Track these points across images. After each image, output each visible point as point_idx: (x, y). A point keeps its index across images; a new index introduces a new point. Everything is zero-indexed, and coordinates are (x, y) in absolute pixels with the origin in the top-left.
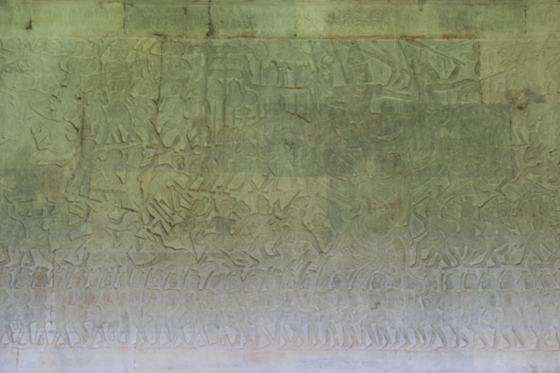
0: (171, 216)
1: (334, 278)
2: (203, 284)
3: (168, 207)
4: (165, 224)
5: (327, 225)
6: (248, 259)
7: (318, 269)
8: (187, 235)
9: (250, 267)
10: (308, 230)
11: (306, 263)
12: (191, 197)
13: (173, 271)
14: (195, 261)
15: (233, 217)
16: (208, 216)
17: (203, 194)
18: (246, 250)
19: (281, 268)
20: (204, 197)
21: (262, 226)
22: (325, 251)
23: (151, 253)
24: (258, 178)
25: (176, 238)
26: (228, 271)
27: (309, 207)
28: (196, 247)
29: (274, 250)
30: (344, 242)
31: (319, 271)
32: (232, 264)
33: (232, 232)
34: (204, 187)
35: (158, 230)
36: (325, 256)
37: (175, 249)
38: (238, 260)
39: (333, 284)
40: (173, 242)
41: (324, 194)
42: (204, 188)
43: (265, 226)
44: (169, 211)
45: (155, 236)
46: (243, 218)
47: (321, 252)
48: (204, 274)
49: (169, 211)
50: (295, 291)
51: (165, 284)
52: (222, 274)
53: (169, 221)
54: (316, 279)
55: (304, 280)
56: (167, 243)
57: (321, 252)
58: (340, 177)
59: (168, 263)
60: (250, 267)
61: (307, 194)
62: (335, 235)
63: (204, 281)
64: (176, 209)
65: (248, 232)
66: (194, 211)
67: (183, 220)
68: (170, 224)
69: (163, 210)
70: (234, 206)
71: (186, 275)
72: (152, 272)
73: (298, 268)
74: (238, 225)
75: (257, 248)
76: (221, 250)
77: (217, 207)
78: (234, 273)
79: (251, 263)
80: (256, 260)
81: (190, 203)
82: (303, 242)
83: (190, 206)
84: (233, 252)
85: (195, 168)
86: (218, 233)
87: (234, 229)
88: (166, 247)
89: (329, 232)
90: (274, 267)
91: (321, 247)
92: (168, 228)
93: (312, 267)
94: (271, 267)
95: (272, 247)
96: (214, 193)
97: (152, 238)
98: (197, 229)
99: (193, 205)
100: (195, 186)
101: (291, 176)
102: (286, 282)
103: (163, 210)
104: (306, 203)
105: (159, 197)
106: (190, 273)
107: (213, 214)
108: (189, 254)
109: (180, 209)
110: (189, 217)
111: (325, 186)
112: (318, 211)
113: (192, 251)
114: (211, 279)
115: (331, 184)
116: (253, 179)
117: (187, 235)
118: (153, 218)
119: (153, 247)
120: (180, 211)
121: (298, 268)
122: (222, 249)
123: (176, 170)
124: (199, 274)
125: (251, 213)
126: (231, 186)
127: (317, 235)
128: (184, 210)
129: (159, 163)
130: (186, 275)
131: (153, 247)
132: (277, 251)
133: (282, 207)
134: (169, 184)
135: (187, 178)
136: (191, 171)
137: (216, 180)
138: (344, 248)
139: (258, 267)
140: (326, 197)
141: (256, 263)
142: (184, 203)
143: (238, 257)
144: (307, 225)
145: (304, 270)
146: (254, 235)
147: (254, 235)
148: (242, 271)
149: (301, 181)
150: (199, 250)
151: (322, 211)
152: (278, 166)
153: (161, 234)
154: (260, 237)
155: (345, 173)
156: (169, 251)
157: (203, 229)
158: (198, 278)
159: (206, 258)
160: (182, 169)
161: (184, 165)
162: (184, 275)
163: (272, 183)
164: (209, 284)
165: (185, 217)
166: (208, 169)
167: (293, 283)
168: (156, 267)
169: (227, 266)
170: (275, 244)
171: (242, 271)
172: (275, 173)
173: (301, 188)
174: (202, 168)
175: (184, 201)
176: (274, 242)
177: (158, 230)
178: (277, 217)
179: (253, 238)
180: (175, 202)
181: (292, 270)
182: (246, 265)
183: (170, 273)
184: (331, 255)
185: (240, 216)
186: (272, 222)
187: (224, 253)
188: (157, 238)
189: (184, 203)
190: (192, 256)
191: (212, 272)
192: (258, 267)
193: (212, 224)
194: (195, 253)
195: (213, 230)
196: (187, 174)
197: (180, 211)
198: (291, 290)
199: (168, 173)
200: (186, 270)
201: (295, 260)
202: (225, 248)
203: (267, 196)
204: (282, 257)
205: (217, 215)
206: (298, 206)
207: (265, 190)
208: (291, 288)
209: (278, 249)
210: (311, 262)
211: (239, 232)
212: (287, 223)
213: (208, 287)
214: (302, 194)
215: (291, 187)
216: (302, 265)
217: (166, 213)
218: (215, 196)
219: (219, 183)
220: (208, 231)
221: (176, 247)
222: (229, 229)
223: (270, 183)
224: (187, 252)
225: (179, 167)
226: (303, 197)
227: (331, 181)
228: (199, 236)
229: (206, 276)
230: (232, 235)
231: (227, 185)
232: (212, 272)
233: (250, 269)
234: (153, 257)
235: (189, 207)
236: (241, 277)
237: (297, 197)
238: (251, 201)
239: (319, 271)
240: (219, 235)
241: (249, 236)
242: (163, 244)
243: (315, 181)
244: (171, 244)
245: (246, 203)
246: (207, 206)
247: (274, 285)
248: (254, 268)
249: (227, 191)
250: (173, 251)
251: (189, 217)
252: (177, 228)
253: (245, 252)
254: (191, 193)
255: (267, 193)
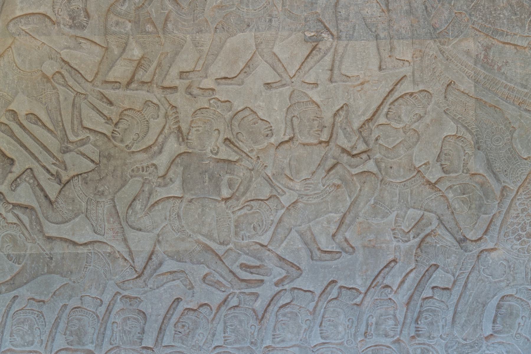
0: (59, 156)
1: (499, 307)
2: (155, 334)
3: (49, 130)
4: (43, 177)
5: (477, 166)
6: (271, 264)
7: (454, 283)
8: (104, 208)
9: (276, 284)
10: (429, 183)
11: (423, 270)
12: (111, 103)
13: (74, 302)
14: (130, 275)
15: (225, 153)
16: (160, 152)
17: (143, 94)
18: (264, 239)
19: (359, 283)
20: (147, 103)
21: (304, 175)
22: (470, 235)
23: (8, 256)
24: (288, 48)
25: (76, 215)
26: (219, 296)
27: (427, 120)
28: (131, 234)
29: (339, 238)
30: (523, 210)
31: (457, 290)
32: (231, 277)
33: (226, 193)
34: (141, 75)
35: (24, 195)
36: (475, 249)
37: (75, 244)
38: (244, 267)
39: (494, 322)
40: (68, 226)
41: (466, 85)
42: (146, 78)
43: (313, 173)
44: (52, 143)
45: (17, 211)
46: (253, 155)
47: (462, 241)
48: (155, 304)
49: (52, 143)
50: (398, 341)
51: (52, 338)
52: (202, 305)
53: (53, 169)
54: (452, 309)
55: (420, 312)
56: (52, 230)
57: (462, 241)
58: (508, 39)
59: (58, 281)
60: (276, 284)
61: (421, 87)
62: (498, 194)
63: (157, 326)
64: (72, 138)
65: (267, 192)
66: (122, 141)
67: (92, 166)
68: (57, 177)
69: (35, 139)
70: (230, 124)
71: (109, 311)
72: (16, 307)
73: (403, 282)
74: (241, 173)
75: (294, 233)
76: (198, 242)
77: (184, 128)
78: (234, 302)
79: (278, 272)
80: (293, 265)
81: (109, 120)
82: (414, 213)
83: (111, 127)
84: (231, 246)
85: (117, 24)
86: (188, 197)
87: (230, 185)
88: (50, 239)
89: (482, 185)
90: (341, 283)
91: (461, 224)
92: (52, 189)
93: (439, 278)
94: (334, 282)
95: (333, 229)
96: (174, 89)
97: (11, 218)
98: (132, 188)
99: (116, 124)
100: (120, 71)
101: (377, 37)
102: (374, 320)
103: (35, 139)
104: (421, 112)
105: (22, 106)
106: (119, 305)
107: (173, 146)
108: (112, 256)
109: (83, 135)
110: (109, 157)
111: (471, 63)
112: (451, 129)
113: (120, 248)
114: (174, 320)
115: (486, 57)
116: (276, 50)
117: (104, 208)
118: (12, 161)
119: (14, 240)
120: (83, 142)
121: (403, 282)
122: (200, 237)
123: (67, 30)
124: (142, 307)
125: (272, 140)
126: (218, 70)
127: (450, 195)
128: (92, 137)
129: (18, 13)
130: (109, 311)
131: (14, 240)
132: (346, 240)
133: (356, 125)
134: (50, 68)
135: (97, 50)
136: (106, 32)
137: (177, 54)
138: (523, 229)
139: (297, 284)
140: (472, 93)
141: (294, 272)
142: (93, 120)
143: (244, 259)
144: (422, 169)
145: (419, 285)
146: (285, 200)
147: (285, 200)
148: (256, 295)
149: (405, 51)
150: (141, 243)
151: (463, 132)
152: (343, 12)
153: (35, 205)
154: (300, 205)
155: (523, 25)
156: (59, 249)
157: (146, 189)
158: (140, 317)
159: (161, 264)
160: (83, 27)
161: (88, 16)
162: (103, 309)
163: (328, 59)
164: (170, 331)
165: (96, 158)
166: (153, 24)
167: (391, 322)
168: (25, 292)
169: (217, 284)
170: (342, 222)
171: (256, 295)
172: (335, 33)
173: (407, 70)
174: (136, 22)
175: (93, 114)
176: (337, 217)
177: (24, 195)
178: (344, 150)
179: (283, 207)
180: (67, 118)
181: (387, 286)
182: (265, 278)
183: (65, 306)
184: (491, 245)
185: (246, 150)
186: (330, 162)
187: (207, 249)
188: (25, 219)
189: (93, 120)
190: (121, 262)
191: (178, 300)
192: (297, 284)
193: (171, 174)
194: (130, 253)
195: (175, 189)
196: (96, 39)
197: (83, 142)
198: (387, 341)
199: (43, 39)
200: (107, 298)
201: (395, 261)
202: (209, 236)
203: (314, 95)
204: (360, 255)
205: (183, 149)
206: (399, 119)
207: (311, 79)
208: (386, 336)
209: (348, 235)
210: (437, 266)
211: (244, 193)
212: (370, 166)
213: (167, 340)
214: (406, 87)
215: (380, 68)
216: (412, 275)
217: (45, 148)
218: (179, 99)
219: (185, 62)
220: (161, 193)
221: (76, 239)
222: (217, 188)
223: (322, 57)
224: (109, 250)
225: (76, 23)
226: (411, 94)
227: (487, 48)
228: (138, 206)
229: (163, 312)
230: (226, 200)
231: (206, 67)
232: (178, 300)
233: (277, 289)
234: (17, 267)
235: (106, 129)
236: (254, 310)
237: (396, 95)
238: (273, 109)
239: (457, 290)
240: (191, 201)
241: (272, 203)
242: (41, 231)
243: (442, 52)
244: (64, 231)
245: (260, 114)
246: (156, 125)
247: (341, 329)
248: (287, 287)
249: (208, 83)
250: (71, 249)
251: (109, 157)
252: (77, 189)
253: (262, 245)
254: (110, 93)
255: (316, 85)
